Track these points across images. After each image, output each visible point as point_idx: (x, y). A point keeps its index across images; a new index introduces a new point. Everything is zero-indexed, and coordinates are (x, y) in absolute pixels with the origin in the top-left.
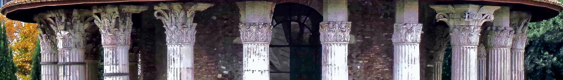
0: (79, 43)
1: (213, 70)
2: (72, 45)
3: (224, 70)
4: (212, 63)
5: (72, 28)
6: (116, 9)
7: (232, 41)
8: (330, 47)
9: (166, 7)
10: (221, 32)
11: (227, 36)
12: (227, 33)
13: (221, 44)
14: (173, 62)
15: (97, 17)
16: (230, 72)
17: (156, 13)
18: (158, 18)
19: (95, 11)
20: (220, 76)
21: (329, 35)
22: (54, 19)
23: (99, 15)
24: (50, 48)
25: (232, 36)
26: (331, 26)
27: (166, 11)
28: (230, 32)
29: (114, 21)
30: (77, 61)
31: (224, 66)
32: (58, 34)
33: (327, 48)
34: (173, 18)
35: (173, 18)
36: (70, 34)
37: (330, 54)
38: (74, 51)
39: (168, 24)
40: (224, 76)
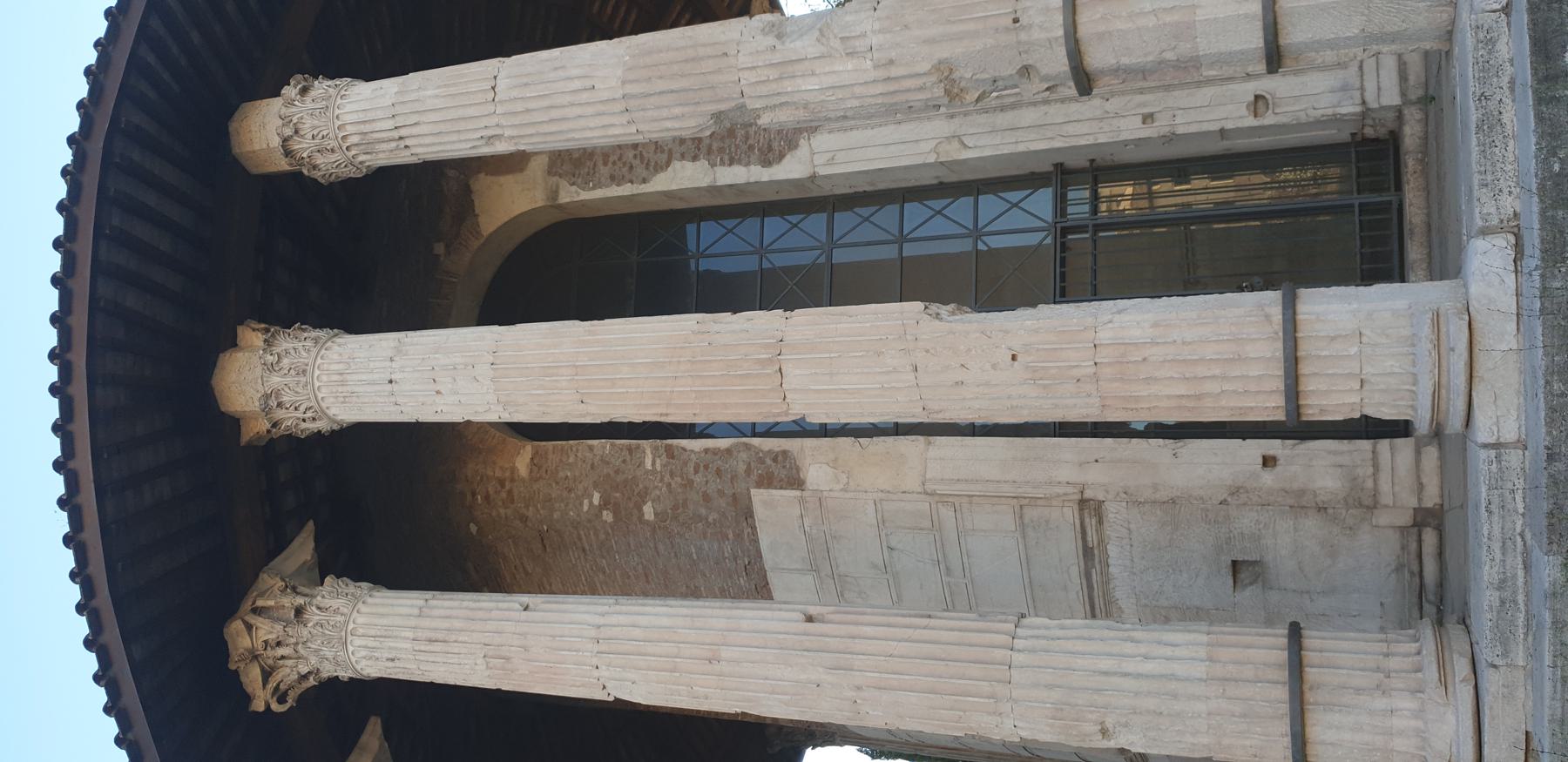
1: (596, 535)
3: (591, 503)
4: (580, 539)
7: (523, 480)
8: (350, 129)
9: (252, 677)
10: (502, 511)
11: (510, 492)
12: (504, 495)
13: (530, 513)
14: (397, 664)
16: (596, 486)
17: (275, 707)
18: (290, 702)
20: (607, 516)
25: (512, 480)
27: (267, 675)
28: (503, 486)
31: (581, 504)
33: (355, 139)
34: (281, 651)
35: (281, 651)
37: (367, 128)
39: (304, 670)
40: (605, 504)
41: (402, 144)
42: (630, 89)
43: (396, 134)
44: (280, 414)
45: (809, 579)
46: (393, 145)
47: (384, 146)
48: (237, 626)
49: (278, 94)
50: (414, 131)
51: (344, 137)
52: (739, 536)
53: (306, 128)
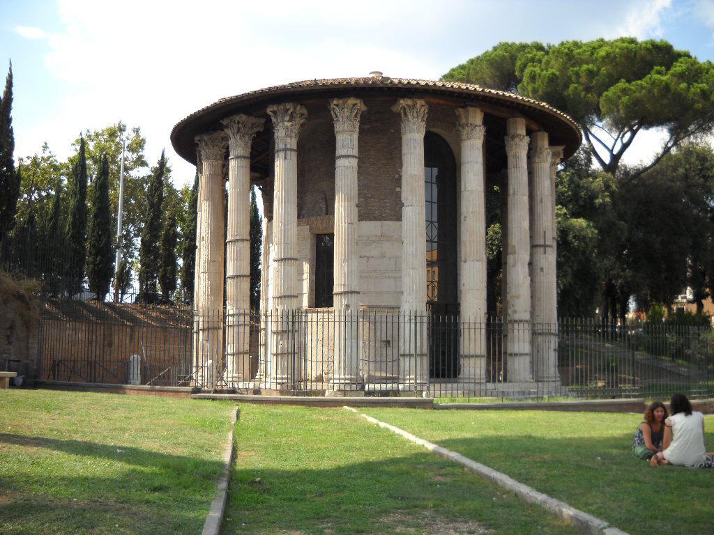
2: (293, 135)
6: (358, 101)
9: (409, 102)
15: (336, 107)
19: (335, 102)
22: (274, 112)
23: (337, 105)
24: (243, 145)
29: (356, 111)
32: (281, 124)
36: (292, 125)
44: (470, 128)
45: (379, 234)
48: (423, 103)
52: (391, 215)
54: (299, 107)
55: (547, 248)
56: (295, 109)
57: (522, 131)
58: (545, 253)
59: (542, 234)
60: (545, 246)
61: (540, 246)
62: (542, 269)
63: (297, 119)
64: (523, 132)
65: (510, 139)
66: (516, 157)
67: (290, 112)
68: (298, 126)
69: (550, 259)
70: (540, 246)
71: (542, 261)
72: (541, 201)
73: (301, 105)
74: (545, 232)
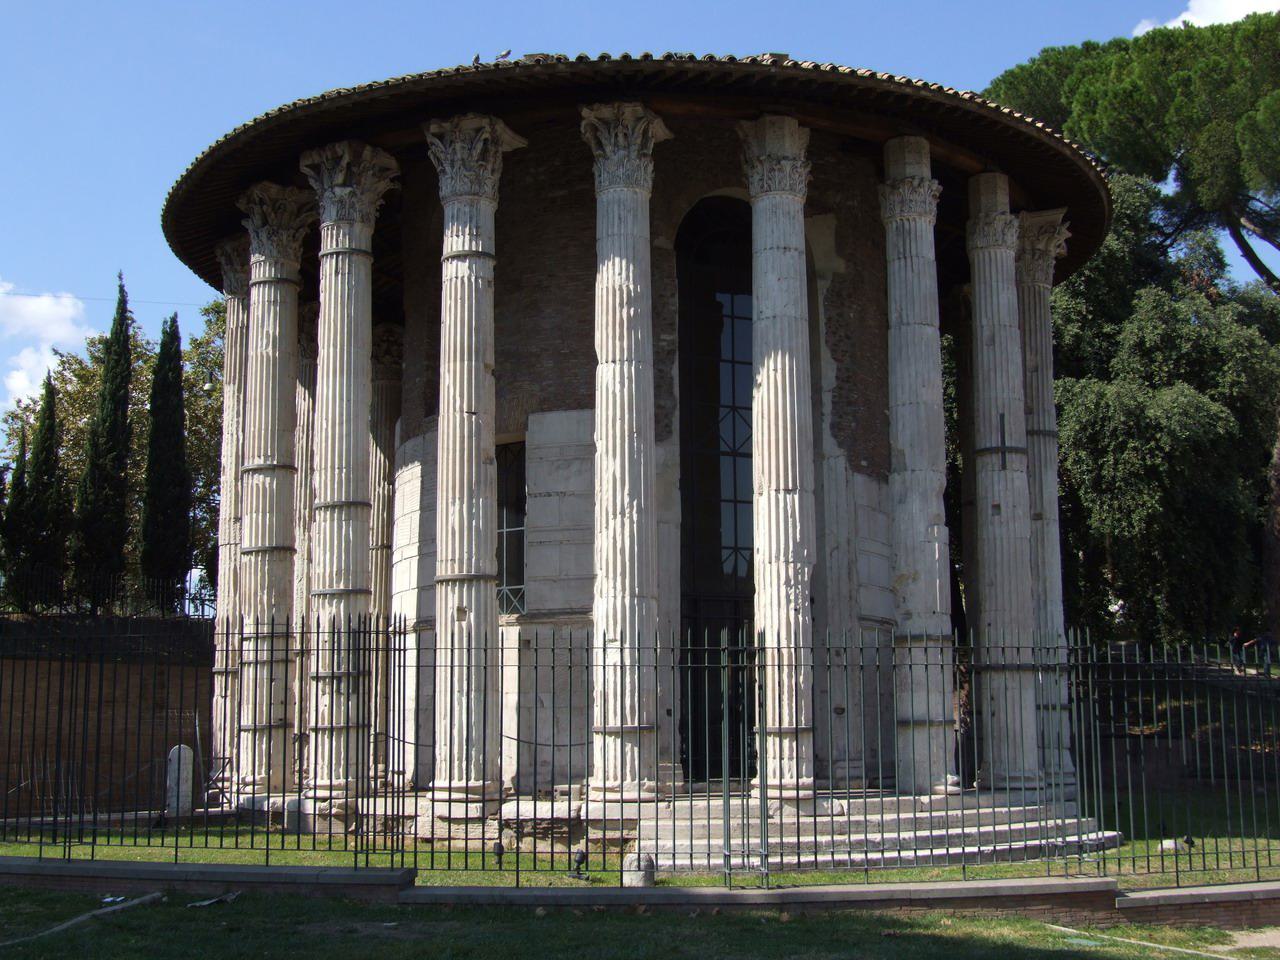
0: (368, 214)
2: (357, 216)
5: (358, 183)
8: (913, 224)
21: (911, 201)
26: (916, 183)
30: (363, 248)
32: (327, 194)
36: (353, 194)
37: (913, 236)
38: (358, 227)
41: (901, 256)
42: (922, 407)
43: (908, 254)
46: (902, 250)
47: (901, 243)
49: (934, 176)
50: (909, 268)
51: (908, 220)
53: (915, 197)
54: (367, 152)
55: (1007, 455)
56: (357, 157)
57: (919, 168)
58: (1004, 467)
59: (995, 421)
60: (1003, 450)
61: (991, 450)
62: (997, 507)
63: (368, 180)
64: (926, 172)
65: (888, 190)
66: (904, 233)
67: (344, 162)
68: (366, 198)
69: (1017, 483)
70: (991, 450)
71: (996, 488)
72: (992, 340)
73: (375, 146)
74: (1002, 416)
